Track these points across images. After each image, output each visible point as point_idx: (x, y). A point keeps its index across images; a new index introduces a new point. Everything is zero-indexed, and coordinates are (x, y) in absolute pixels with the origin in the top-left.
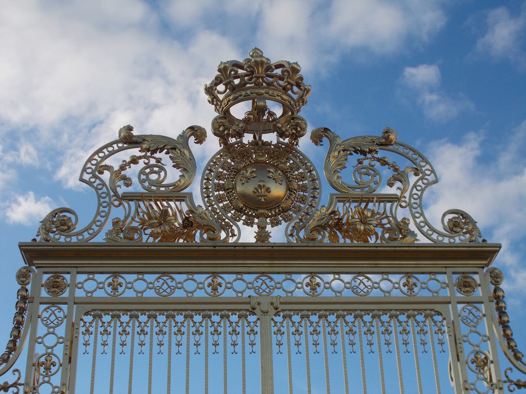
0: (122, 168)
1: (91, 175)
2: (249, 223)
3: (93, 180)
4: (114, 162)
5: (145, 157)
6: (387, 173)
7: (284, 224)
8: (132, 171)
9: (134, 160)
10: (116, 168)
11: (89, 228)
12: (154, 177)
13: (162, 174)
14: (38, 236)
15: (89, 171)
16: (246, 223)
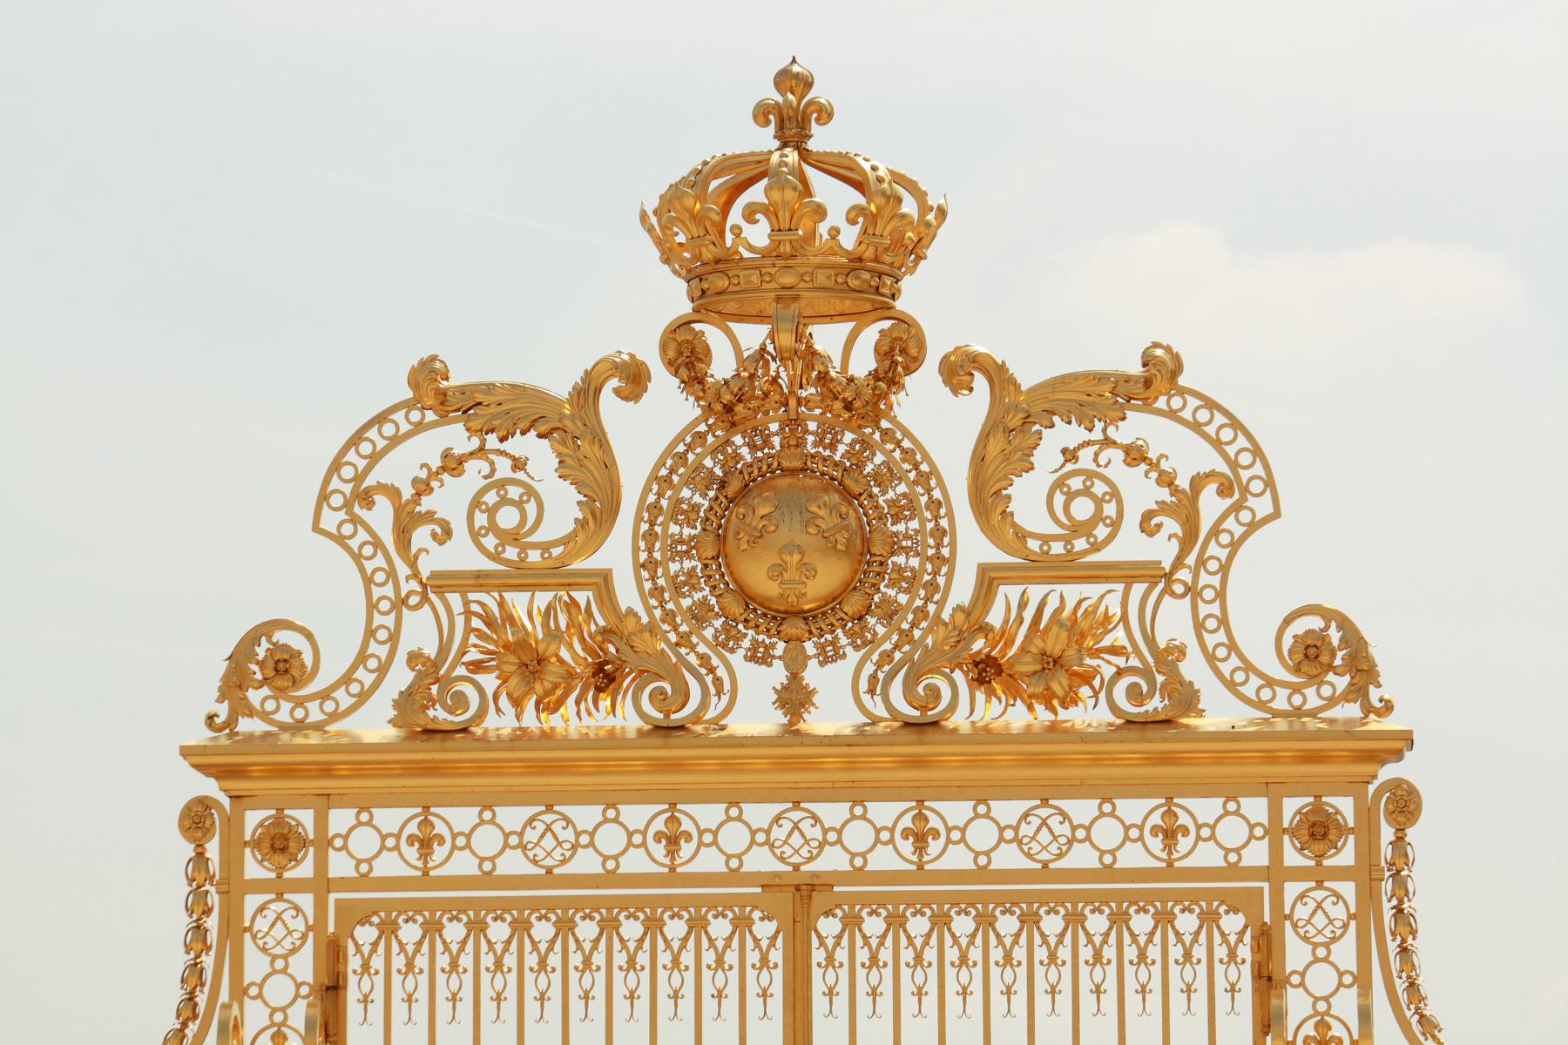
0: (423, 487)
1: (342, 515)
2: (759, 656)
3: (347, 529)
4: (399, 469)
5: (481, 451)
6: (1141, 491)
7: (854, 657)
8: (450, 499)
9: (453, 464)
10: (407, 492)
11: (346, 679)
12: (508, 518)
13: (531, 509)
14: (220, 700)
15: (337, 500)
16: (752, 657)
